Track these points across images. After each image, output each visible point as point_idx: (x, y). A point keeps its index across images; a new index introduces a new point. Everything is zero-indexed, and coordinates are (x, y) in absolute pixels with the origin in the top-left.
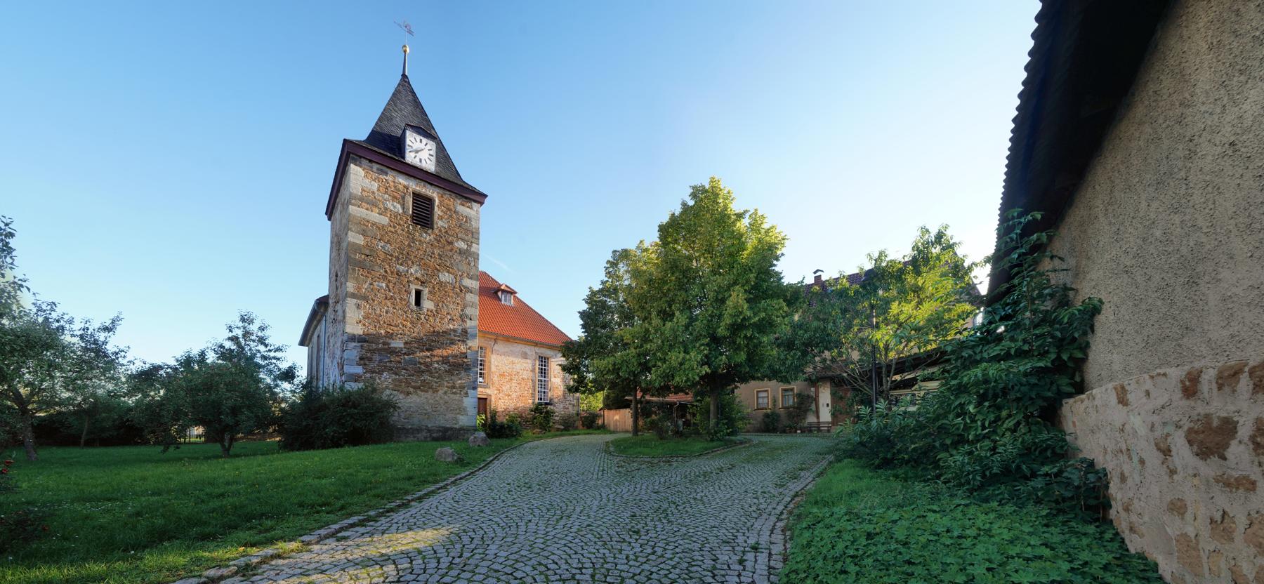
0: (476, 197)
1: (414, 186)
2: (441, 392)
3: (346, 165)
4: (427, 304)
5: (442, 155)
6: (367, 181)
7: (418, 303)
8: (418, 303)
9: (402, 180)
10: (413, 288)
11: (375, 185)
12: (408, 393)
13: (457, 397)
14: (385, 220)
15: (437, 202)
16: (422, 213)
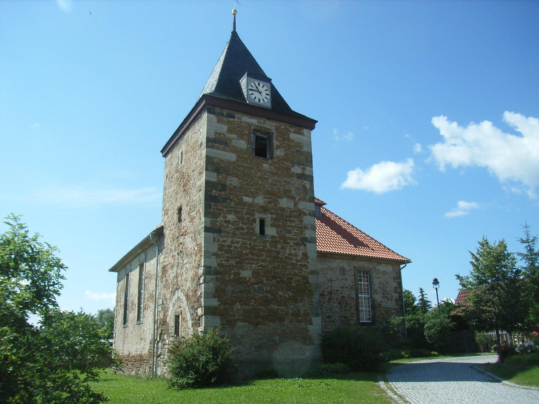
0: (310, 124)
1: (254, 121)
2: (286, 322)
3: (200, 113)
4: (270, 231)
5: (275, 95)
6: (219, 125)
7: (262, 231)
8: (262, 231)
9: (246, 119)
10: (258, 216)
11: (224, 128)
12: (258, 324)
13: (303, 325)
14: (232, 157)
15: (275, 134)
16: (262, 148)
